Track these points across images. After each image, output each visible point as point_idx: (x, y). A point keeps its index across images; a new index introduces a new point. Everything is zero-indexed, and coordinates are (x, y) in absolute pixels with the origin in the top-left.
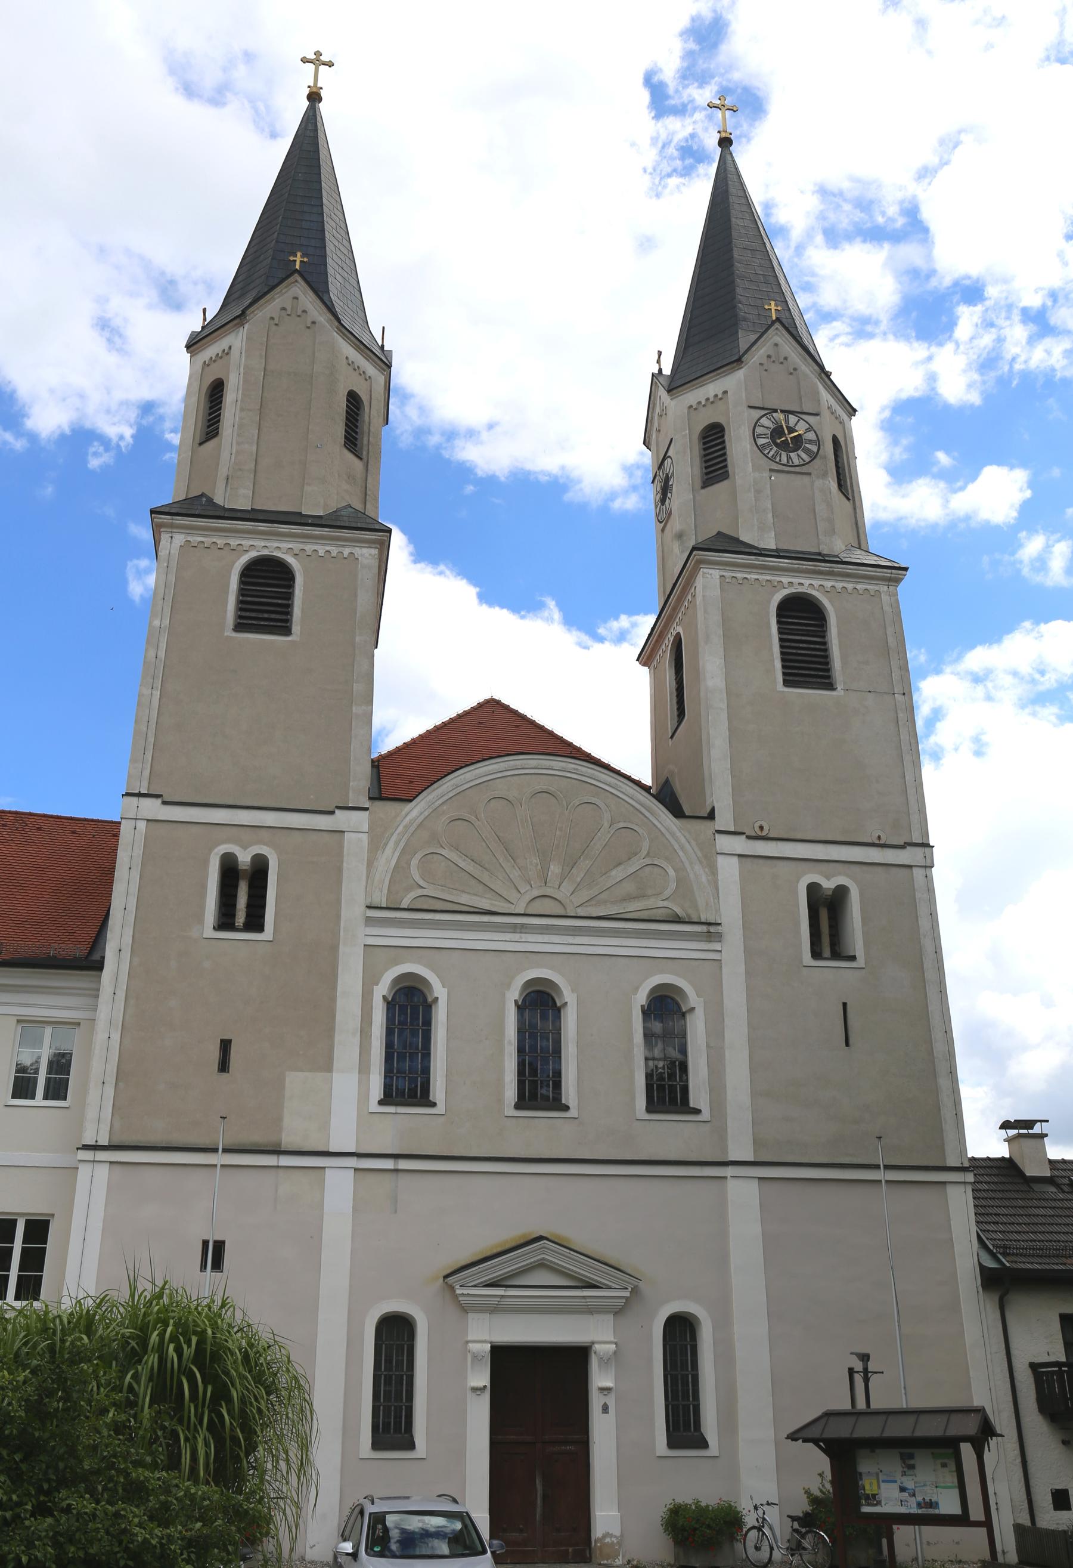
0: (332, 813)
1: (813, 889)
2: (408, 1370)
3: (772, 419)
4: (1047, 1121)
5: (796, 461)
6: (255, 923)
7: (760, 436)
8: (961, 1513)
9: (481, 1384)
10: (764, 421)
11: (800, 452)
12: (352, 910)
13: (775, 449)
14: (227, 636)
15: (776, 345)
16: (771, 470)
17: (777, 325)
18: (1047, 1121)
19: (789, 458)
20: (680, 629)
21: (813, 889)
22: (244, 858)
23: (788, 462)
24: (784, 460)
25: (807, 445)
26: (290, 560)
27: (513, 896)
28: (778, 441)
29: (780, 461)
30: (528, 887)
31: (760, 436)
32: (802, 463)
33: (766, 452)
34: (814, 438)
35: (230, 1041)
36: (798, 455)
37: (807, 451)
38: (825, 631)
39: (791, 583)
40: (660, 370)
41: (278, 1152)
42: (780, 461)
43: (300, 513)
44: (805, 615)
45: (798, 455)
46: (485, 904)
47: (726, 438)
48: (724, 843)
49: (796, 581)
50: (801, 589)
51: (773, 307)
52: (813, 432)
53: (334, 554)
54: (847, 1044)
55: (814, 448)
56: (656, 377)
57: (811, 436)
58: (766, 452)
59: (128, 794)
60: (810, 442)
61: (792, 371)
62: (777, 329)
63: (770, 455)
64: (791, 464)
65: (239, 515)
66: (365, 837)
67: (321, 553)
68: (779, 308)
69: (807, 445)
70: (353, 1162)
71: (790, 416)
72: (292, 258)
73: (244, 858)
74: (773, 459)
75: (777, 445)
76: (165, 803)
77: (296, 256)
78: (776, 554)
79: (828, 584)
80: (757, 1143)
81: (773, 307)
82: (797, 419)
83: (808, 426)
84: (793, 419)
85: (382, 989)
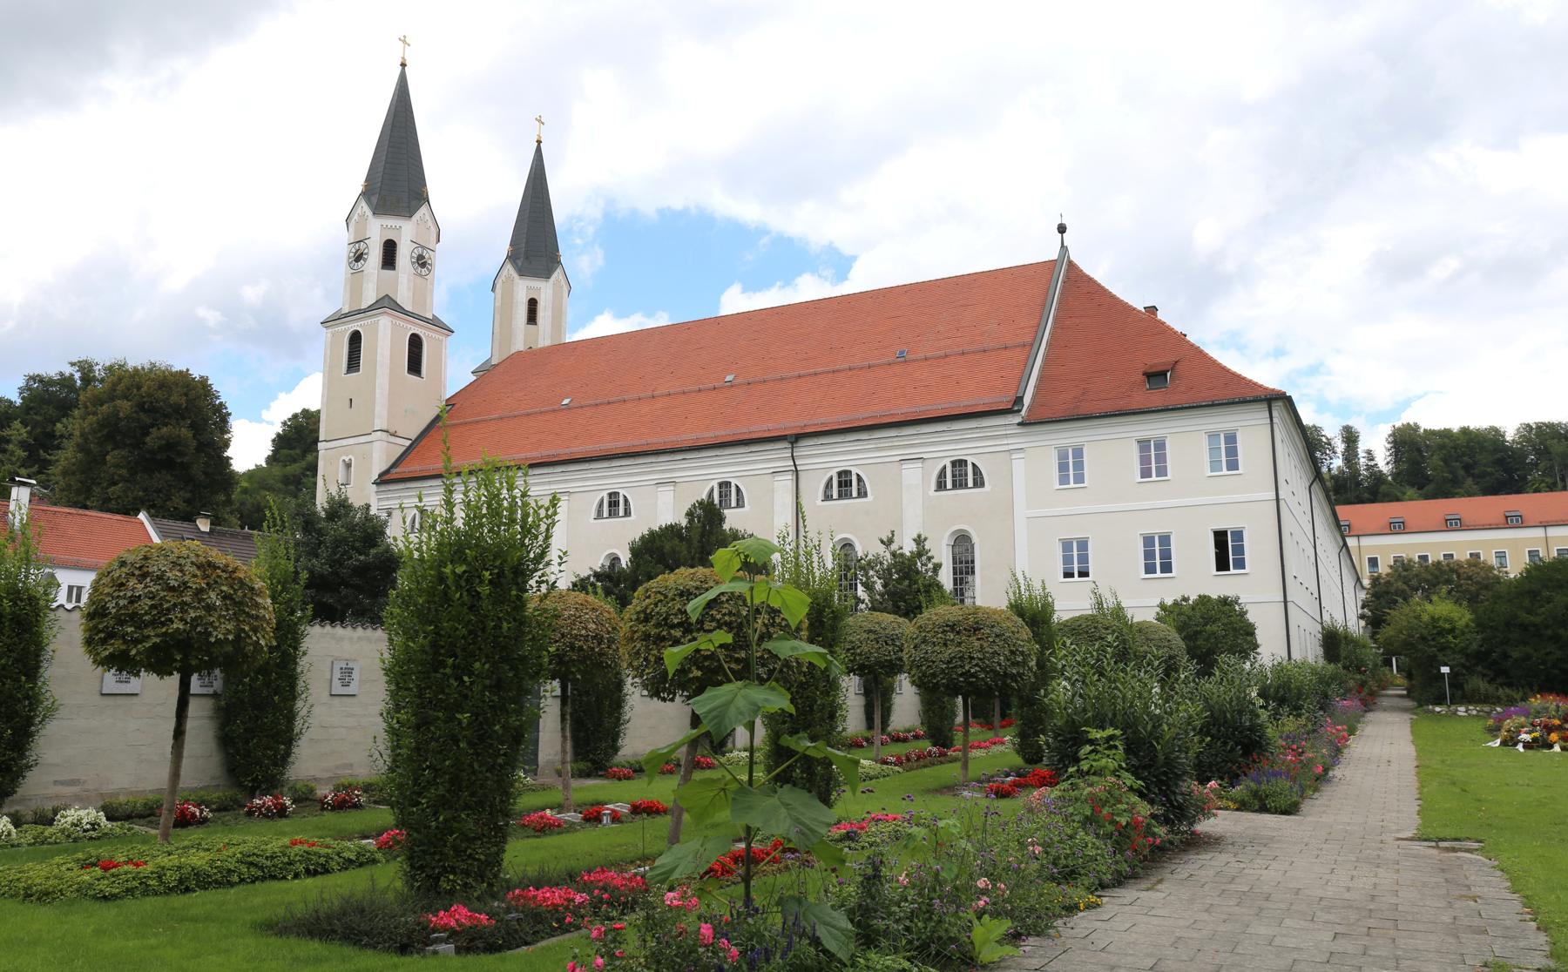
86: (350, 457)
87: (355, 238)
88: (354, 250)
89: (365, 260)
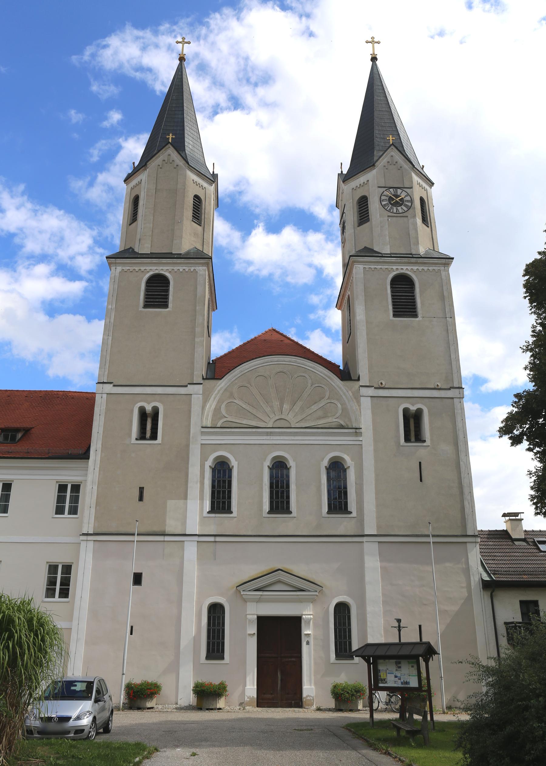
0: (186, 386)
1: (406, 411)
2: (222, 626)
3: (389, 192)
4: (523, 513)
5: (401, 211)
6: (154, 436)
7: (383, 200)
8: (418, 686)
9: (252, 632)
10: (386, 193)
11: (403, 207)
12: (195, 429)
14: (141, 311)
15: (392, 156)
16: (388, 216)
17: (392, 147)
18: (523, 513)
19: (397, 210)
20: (349, 293)
21: (406, 411)
22: (149, 408)
23: (397, 212)
24: (395, 211)
25: (406, 203)
26: (168, 274)
27: (266, 419)
28: (392, 202)
29: (393, 211)
30: (274, 415)
31: (383, 200)
32: (403, 211)
33: (386, 208)
34: (410, 199)
35: (143, 488)
36: (402, 208)
37: (406, 206)
38: (414, 290)
39: (397, 269)
40: (342, 172)
41: (164, 535)
42: (393, 211)
43: (171, 253)
44: (404, 283)
45: (402, 208)
46: (254, 423)
47: (369, 202)
48: (363, 391)
49: (399, 267)
50: (402, 271)
51: (391, 138)
52: (409, 196)
53: (187, 270)
54: (421, 480)
55: (409, 204)
56: (340, 175)
57: (408, 198)
58: (386, 208)
59: (98, 383)
60: (408, 201)
61: (399, 168)
62: (392, 148)
63: (388, 209)
64: (398, 212)
65: (144, 256)
66: (201, 396)
67: (181, 270)
68: (394, 139)
69: (406, 203)
70: (196, 538)
71: (398, 190)
72: (167, 137)
73: (149, 408)
74: (389, 211)
75: (391, 204)
76: (114, 386)
77: (169, 136)
78: (390, 256)
79: (415, 268)
80: (379, 527)
81: (391, 138)
82: (401, 191)
83: (407, 194)
84: (399, 191)
85: (209, 463)
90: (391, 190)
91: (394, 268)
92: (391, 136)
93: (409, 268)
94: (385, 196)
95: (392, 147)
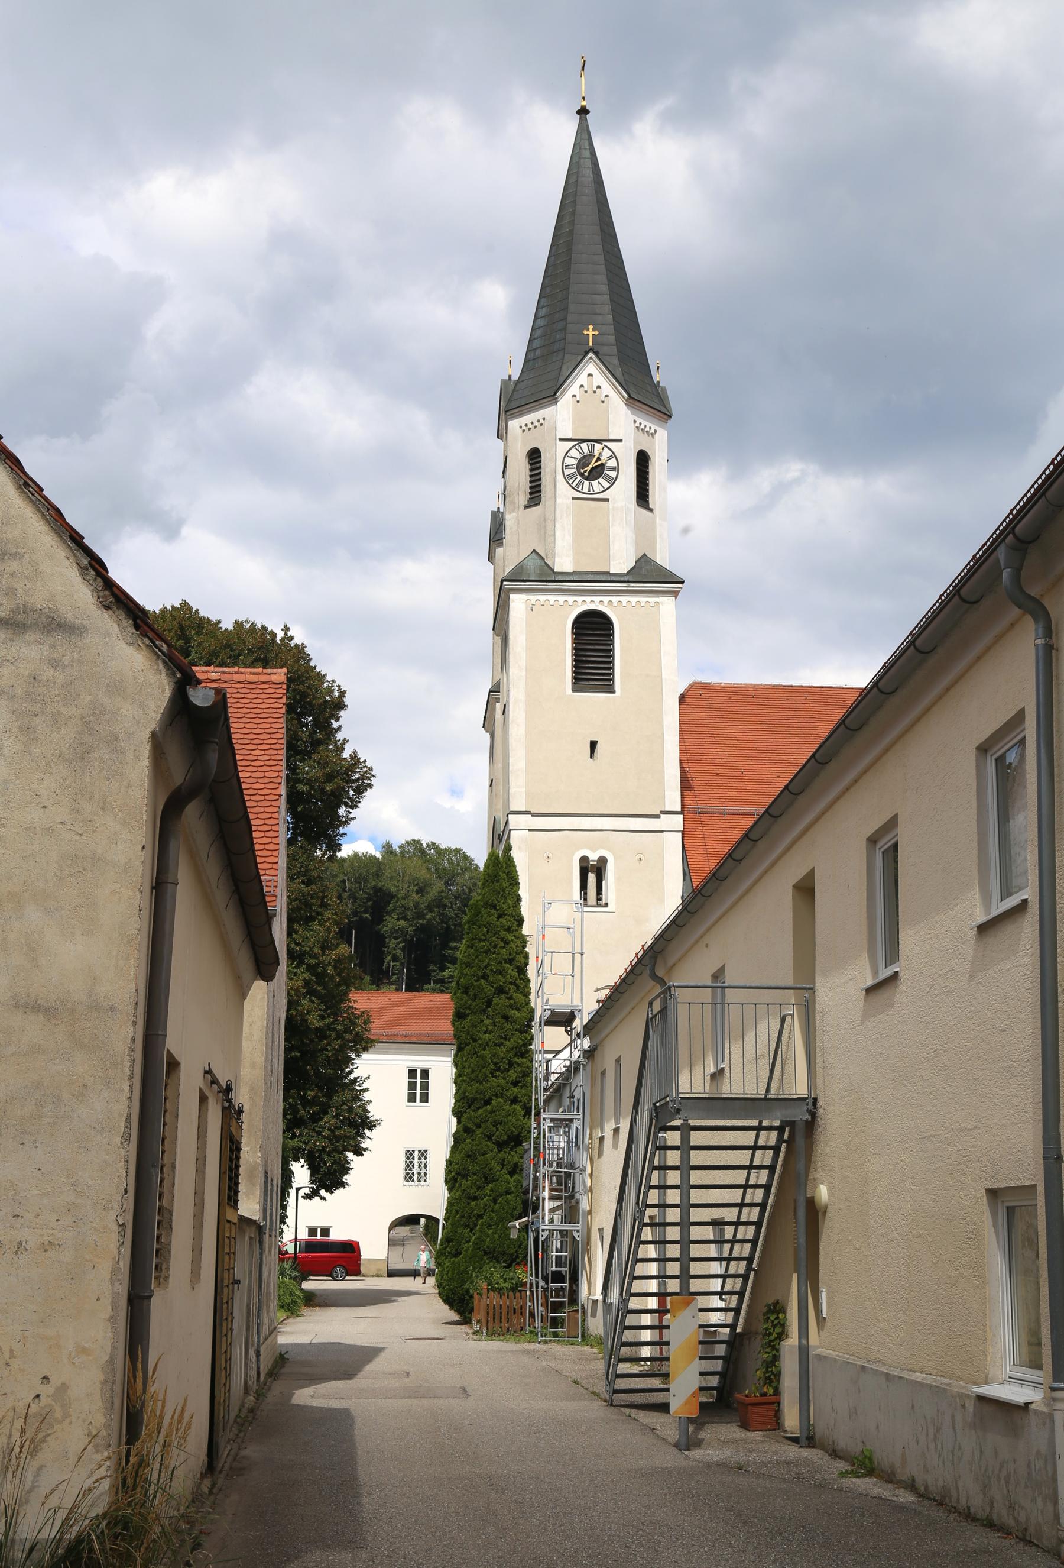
1: (584, 859)
7: (568, 467)
10: (574, 453)
11: (600, 480)
13: (579, 478)
16: (574, 499)
17: (591, 355)
19: (590, 486)
21: (584, 859)
23: (589, 491)
24: (586, 490)
25: (607, 472)
32: (602, 489)
33: (570, 482)
36: (599, 483)
45: (599, 483)
49: (588, 599)
51: (591, 333)
55: (613, 474)
57: (612, 463)
58: (570, 482)
60: (612, 469)
62: (591, 358)
63: (574, 485)
64: (592, 492)
69: (607, 472)
75: (582, 475)
83: (611, 454)
84: (598, 446)
86: (603, 853)
87: (574, 430)
88: (574, 453)
89: (612, 482)
90: (584, 445)
91: (580, 599)
92: (591, 327)
93: (606, 599)
94: (572, 457)
95: (591, 355)
